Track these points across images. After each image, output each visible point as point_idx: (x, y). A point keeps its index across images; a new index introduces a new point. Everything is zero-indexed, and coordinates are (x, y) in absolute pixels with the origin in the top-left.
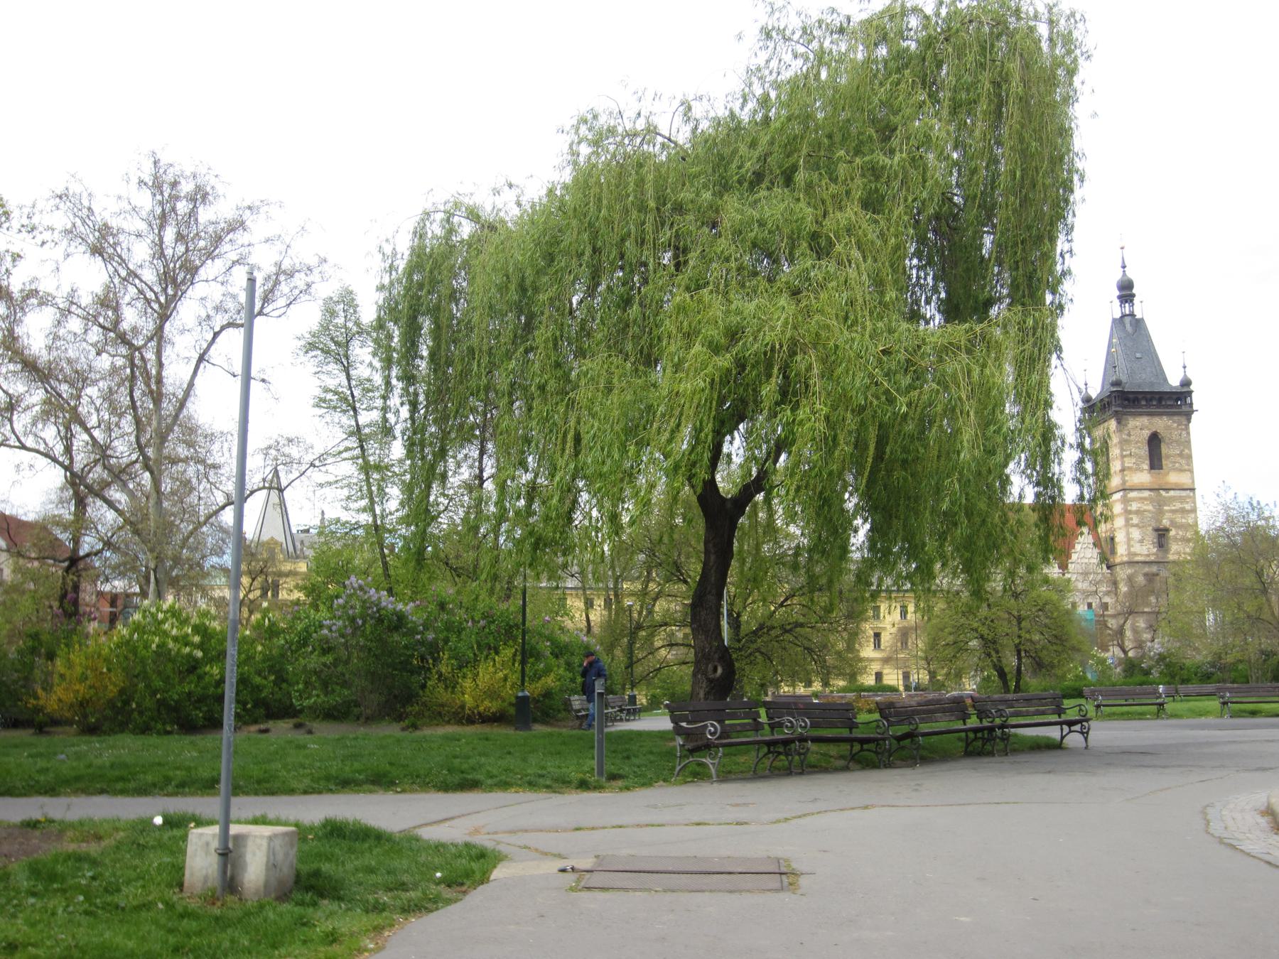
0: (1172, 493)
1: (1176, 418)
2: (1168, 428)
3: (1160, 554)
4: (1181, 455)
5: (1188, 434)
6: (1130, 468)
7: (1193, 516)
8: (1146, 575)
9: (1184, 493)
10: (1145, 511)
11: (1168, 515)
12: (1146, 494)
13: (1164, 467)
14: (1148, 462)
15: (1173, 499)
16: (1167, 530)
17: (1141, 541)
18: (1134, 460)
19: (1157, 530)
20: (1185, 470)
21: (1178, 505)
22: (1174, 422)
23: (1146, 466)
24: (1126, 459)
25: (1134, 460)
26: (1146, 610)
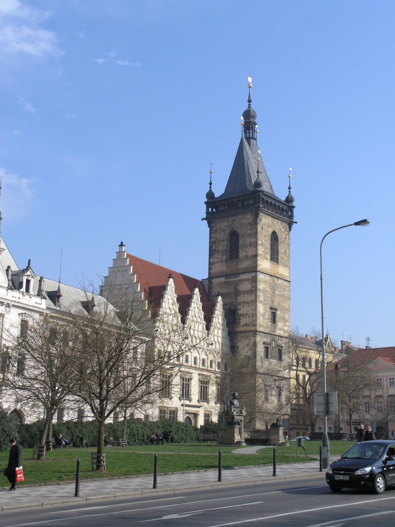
5: (289, 238)
6: (261, 255)
9: (286, 283)
10: (266, 292)
11: (277, 297)
12: (268, 278)
14: (270, 253)
16: (276, 310)
17: (263, 316)
19: (271, 309)
23: (269, 257)
25: (263, 250)
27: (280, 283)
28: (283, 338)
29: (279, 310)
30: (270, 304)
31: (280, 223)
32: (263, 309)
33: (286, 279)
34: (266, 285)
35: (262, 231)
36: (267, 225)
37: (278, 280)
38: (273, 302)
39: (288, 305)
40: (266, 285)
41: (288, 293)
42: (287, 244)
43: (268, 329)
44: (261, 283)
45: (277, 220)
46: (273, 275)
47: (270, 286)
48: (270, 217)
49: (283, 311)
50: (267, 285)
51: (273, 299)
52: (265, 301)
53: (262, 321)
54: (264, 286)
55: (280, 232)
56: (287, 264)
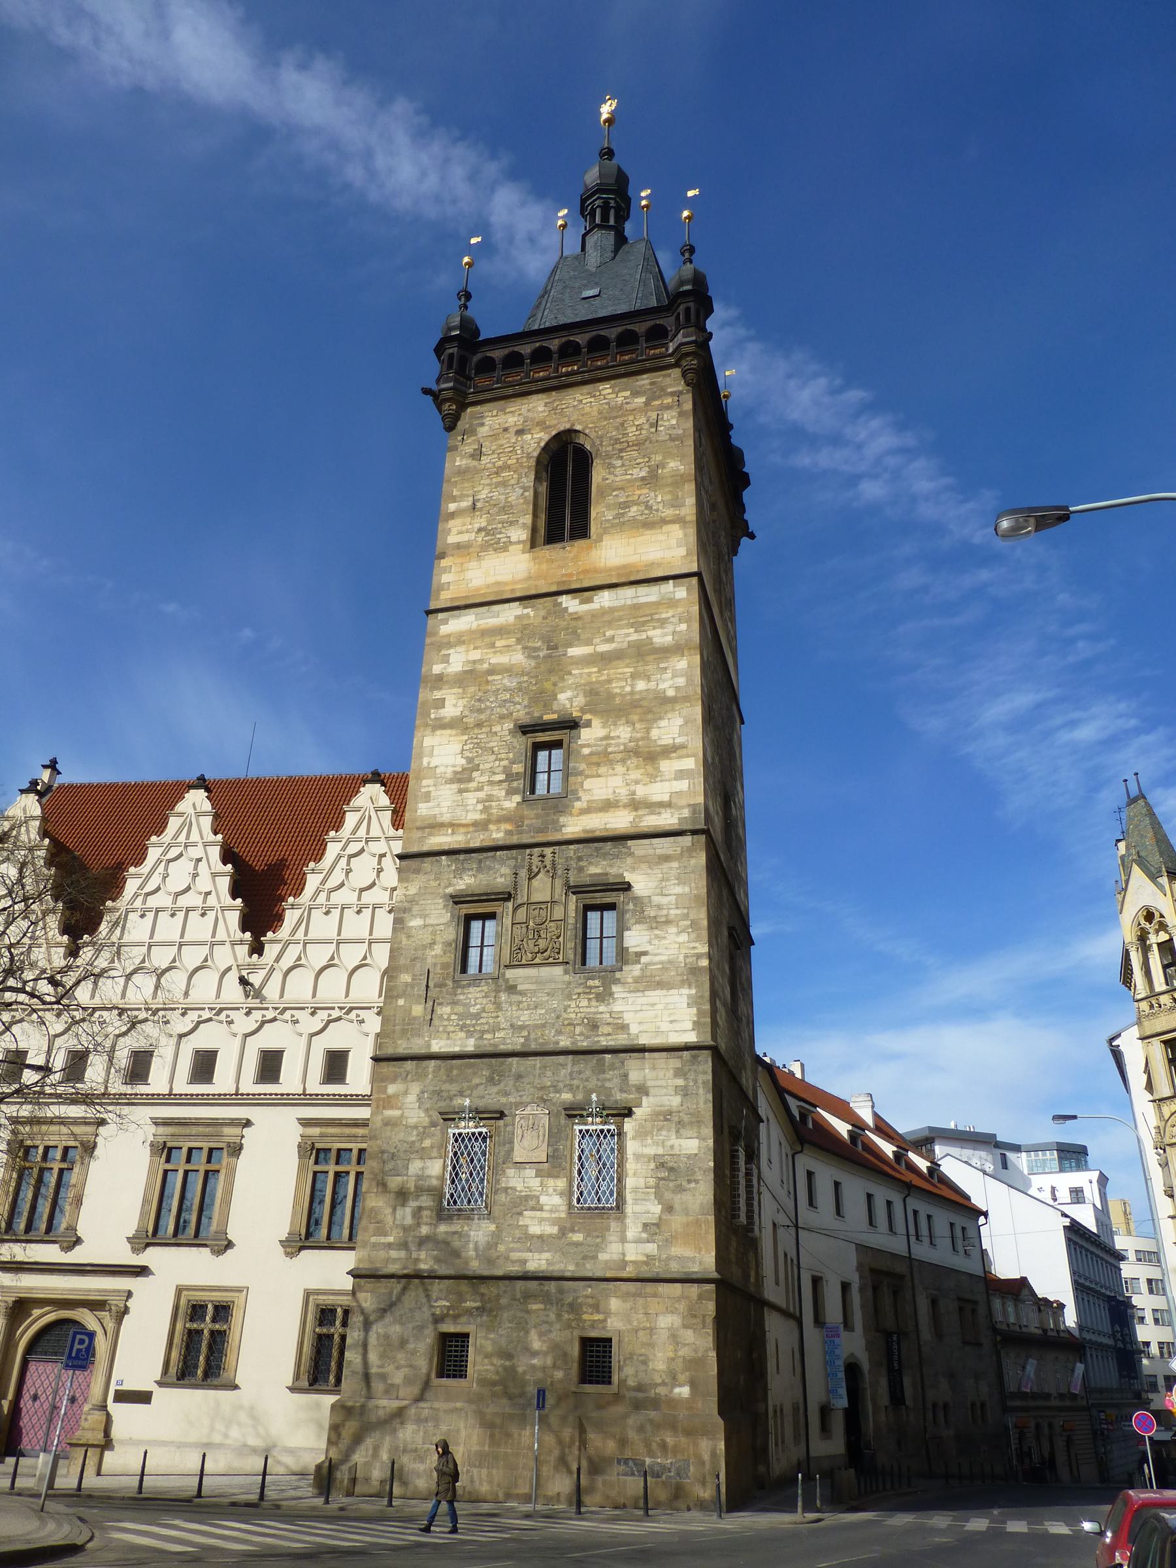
0: (605, 599)
1: (644, 381)
2: (616, 412)
3: (531, 816)
4: (652, 479)
6: (458, 546)
7: (681, 664)
8: (457, 900)
10: (491, 672)
12: (509, 614)
13: (594, 529)
15: (608, 617)
17: (462, 778)
18: (481, 522)
20: (664, 522)
21: (626, 636)
22: (636, 394)
23: (520, 534)
24: (451, 523)
25: (481, 522)
26: (438, 1046)
27: (607, 604)
28: (630, 843)
29: (596, 722)
30: (522, 713)
31: (610, 391)
32: (463, 750)
33: (660, 574)
34: (493, 645)
35: (475, 463)
36: (513, 430)
37: (589, 600)
38: (544, 698)
39: (681, 681)
40: (493, 645)
41: (683, 627)
42: (672, 439)
43: (492, 827)
44: (451, 651)
45: (586, 389)
46: (554, 589)
47: (519, 641)
48: (535, 397)
49: (635, 718)
50: (499, 644)
51: (548, 685)
52: (480, 711)
53: (446, 804)
54: (476, 655)
55: (606, 419)
56: (669, 512)
